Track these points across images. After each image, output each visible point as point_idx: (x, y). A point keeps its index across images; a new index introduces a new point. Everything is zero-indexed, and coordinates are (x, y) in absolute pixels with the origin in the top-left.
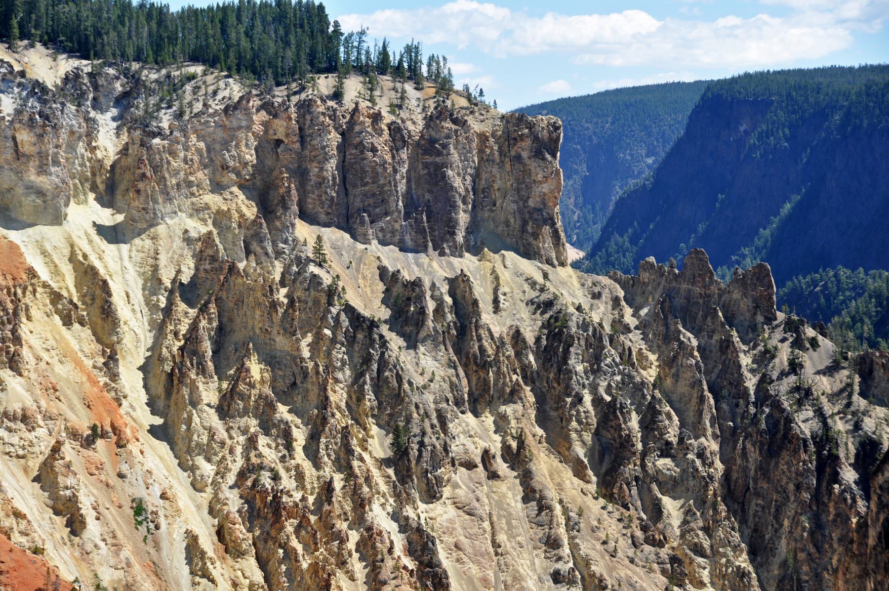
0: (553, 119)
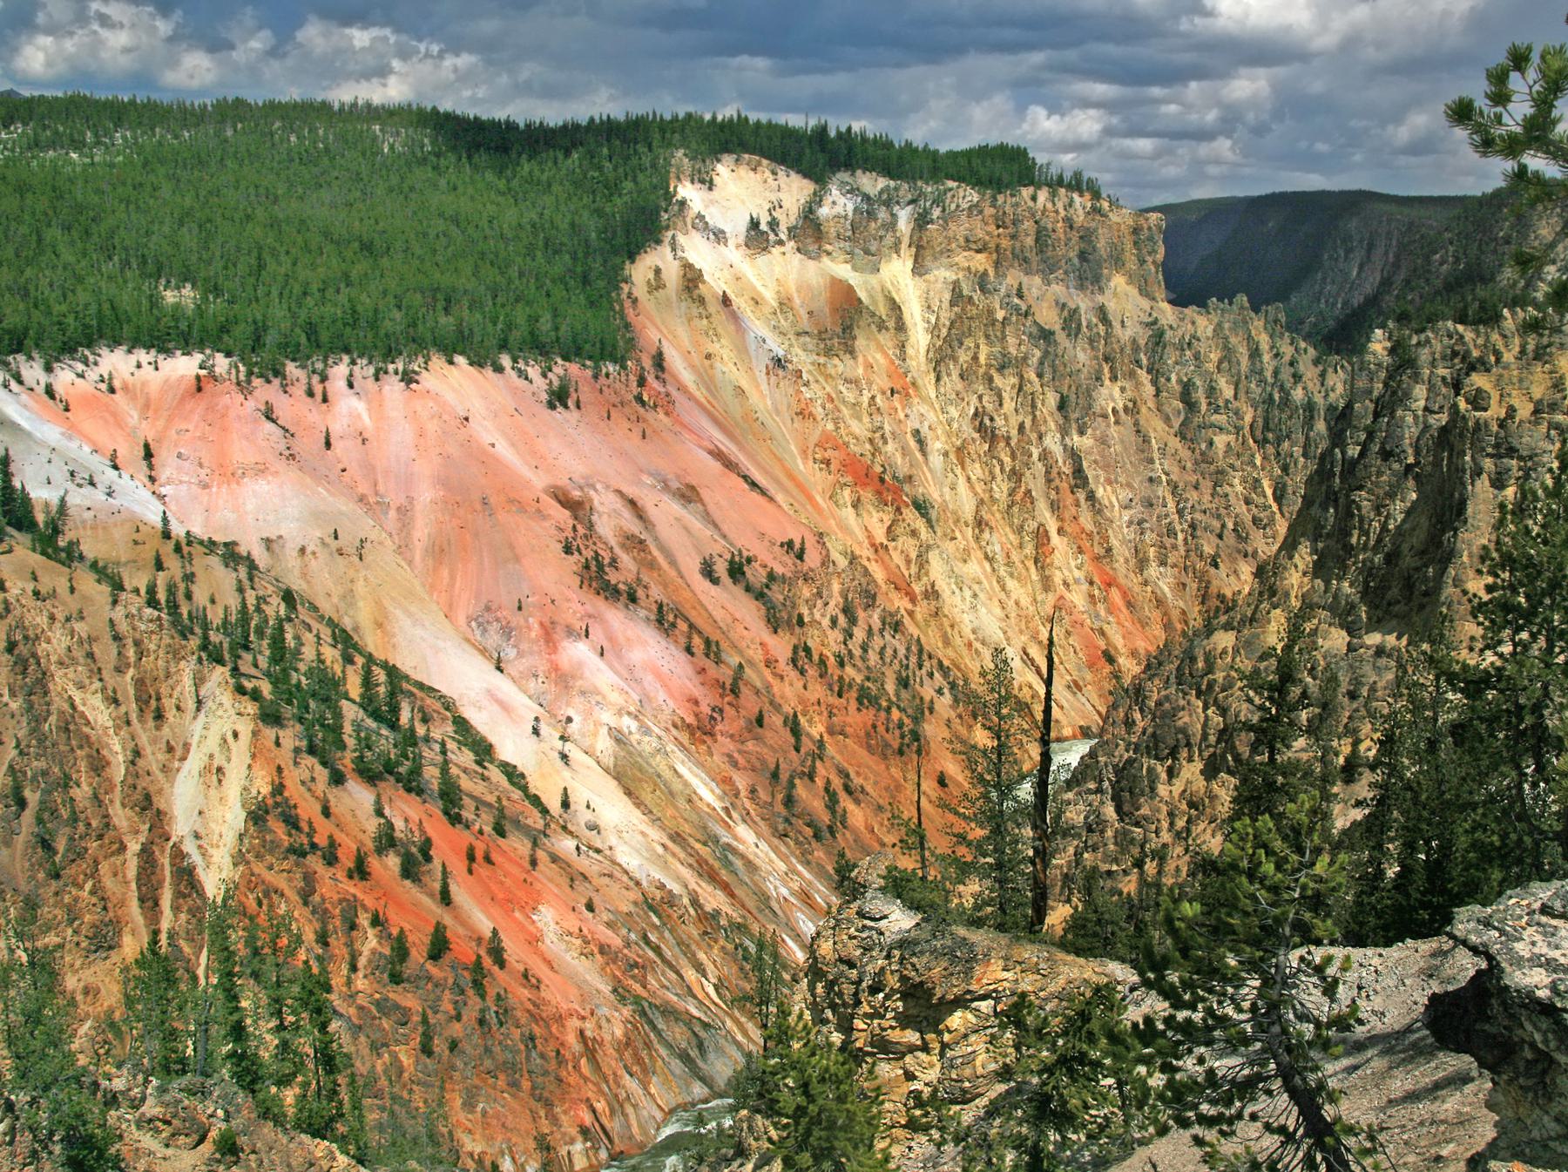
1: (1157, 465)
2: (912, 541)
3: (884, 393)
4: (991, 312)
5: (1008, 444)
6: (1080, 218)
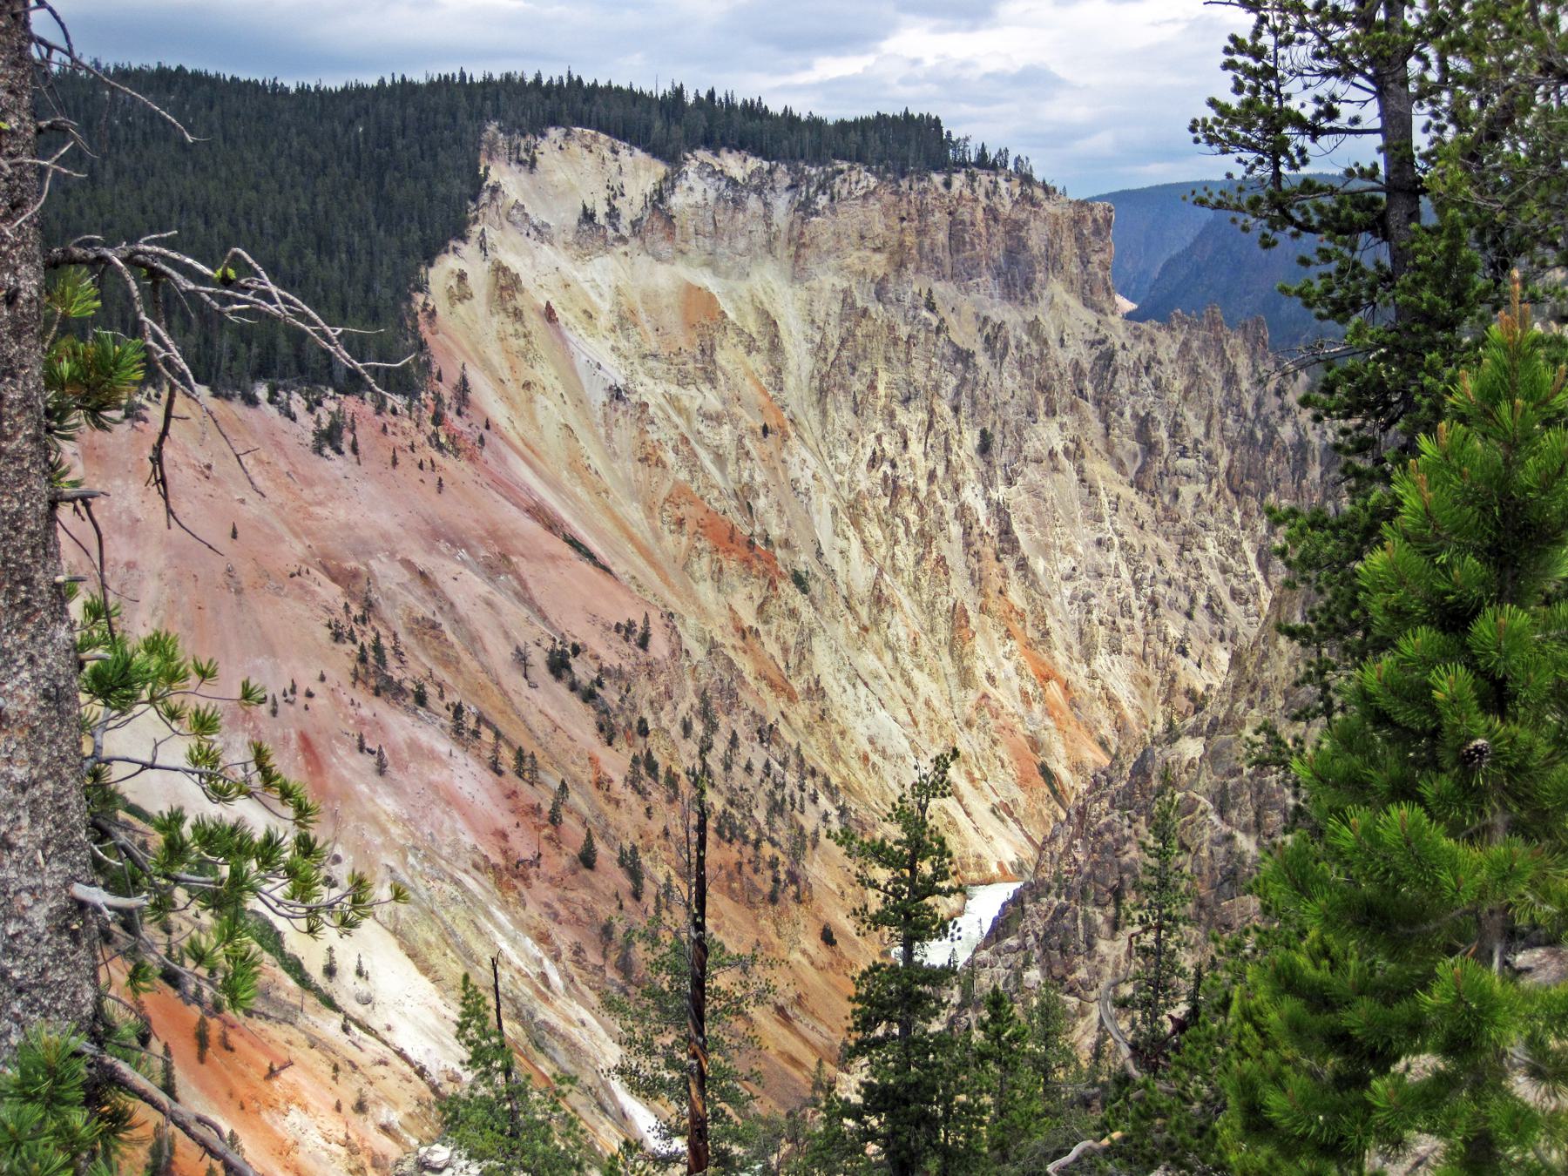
0: (1107, 204)
1: (1107, 524)
2: (789, 624)
3: (753, 432)
4: (891, 328)
5: (915, 497)
6: (1006, 207)
